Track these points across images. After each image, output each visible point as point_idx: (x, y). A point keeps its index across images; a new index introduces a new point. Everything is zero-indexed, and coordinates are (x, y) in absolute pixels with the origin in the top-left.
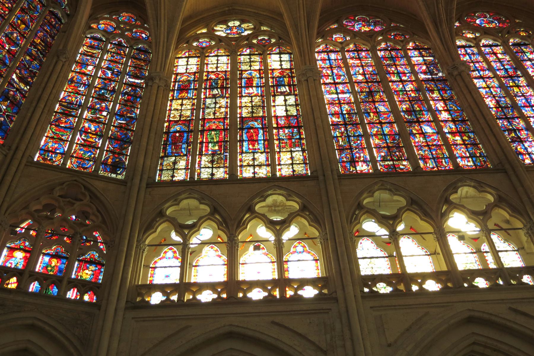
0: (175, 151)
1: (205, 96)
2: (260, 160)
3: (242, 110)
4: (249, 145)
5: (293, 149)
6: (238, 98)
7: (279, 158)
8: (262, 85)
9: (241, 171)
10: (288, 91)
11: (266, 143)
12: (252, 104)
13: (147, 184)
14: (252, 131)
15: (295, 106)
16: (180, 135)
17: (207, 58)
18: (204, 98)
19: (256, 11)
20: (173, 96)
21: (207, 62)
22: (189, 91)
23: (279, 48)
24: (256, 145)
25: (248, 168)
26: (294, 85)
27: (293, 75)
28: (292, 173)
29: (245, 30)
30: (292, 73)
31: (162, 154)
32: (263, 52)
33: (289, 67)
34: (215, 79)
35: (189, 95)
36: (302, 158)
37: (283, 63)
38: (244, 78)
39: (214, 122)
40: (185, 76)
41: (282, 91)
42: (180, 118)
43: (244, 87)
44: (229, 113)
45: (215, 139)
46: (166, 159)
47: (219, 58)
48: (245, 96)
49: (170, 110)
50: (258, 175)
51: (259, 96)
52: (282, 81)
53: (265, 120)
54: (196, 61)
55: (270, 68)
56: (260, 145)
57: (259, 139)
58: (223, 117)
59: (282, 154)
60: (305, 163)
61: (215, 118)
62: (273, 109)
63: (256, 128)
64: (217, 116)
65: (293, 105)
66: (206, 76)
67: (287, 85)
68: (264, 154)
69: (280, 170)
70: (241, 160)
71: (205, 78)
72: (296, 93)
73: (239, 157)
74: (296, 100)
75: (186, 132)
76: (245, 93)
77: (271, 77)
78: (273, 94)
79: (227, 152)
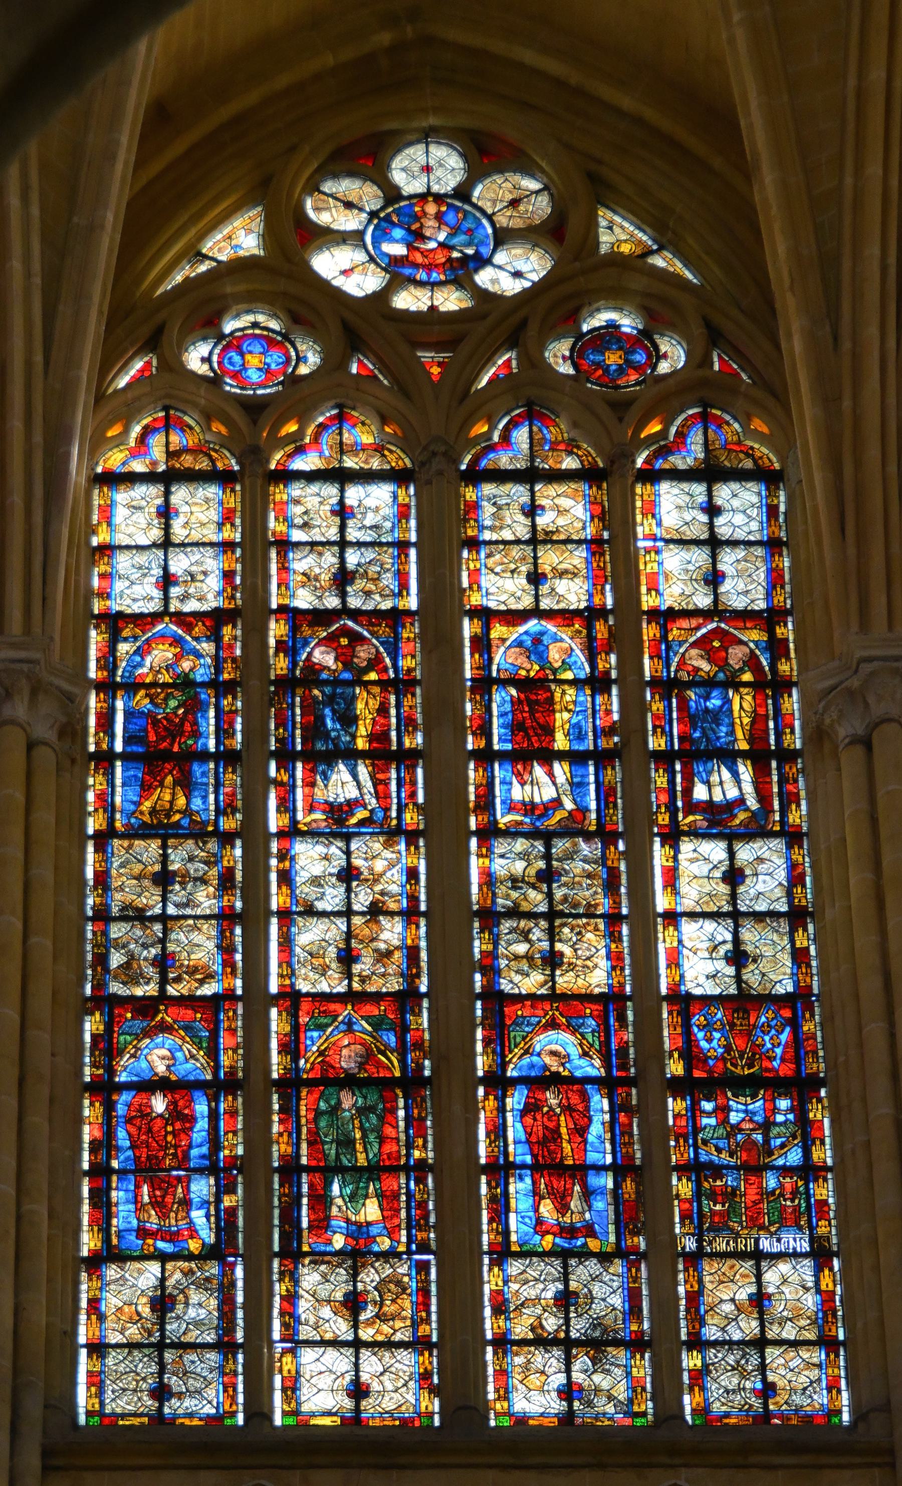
0: (153, 1221)
1: (286, 820)
2: (598, 1308)
3: (496, 944)
4: (536, 1193)
5: (766, 1244)
6: (474, 842)
7: (694, 1298)
8: (603, 743)
9: (502, 1373)
10: (752, 803)
11: (629, 1186)
12: (550, 895)
13: (47, 1453)
14: (552, 1099)
15: (784, 926)
16: (173, 1107)
17: (280, 494)
18: (281, 834)
19: (575, 78)
20: (106, 803)
21: (281, 528)
22: (197, 769)
23: (705, 418)
24: (575, 1204)
25: (539, 1358)
26: (787, 756)
27: (784, 667)
28: (756, 1403)
29: (502, 238)
30: (777, 649)
31: (89, 1242)
32: (611, 461)
33: (761, 605)
34: (337, 682)
35: (197, 803)
36: (810, 1301)
37: (728, 560)
38: (504, 683)
39: (349, 1024)
40: (162, 637)
41: (718, 797)
42: (163, 982)
43: (502, 756)
44: (424, 955)
45: (359, 1147)
46: (111, 1272)
47: (354, 494)
48: (511, 833)
49: (102, 916)
50: (590, 1404)
51: (588, 836)
52: (715, 716)
53: (622, 1019)
54: (214, 515)
55: (648, 601)
56: (599, 1204)
57: (592, 1157)
58: (394, 985)
59: (709, 1267)
60: (827, 1343)
61: (349, 997)
62: (665, 940)
63: (572, 1080)
64: (363, 980)
65: (773, 914)
66: (281, 646)
67: (744, 755)
68: (618, 1266)
69: (699, 1377)
70: (500, 1307)
71: (280, 665)
72: (794, 818)
73: (491, 1281)
74: (795, 879)
75: (200, 1085)
76: (511, 807)
77: (655, 683)
78: (664, 819)
79: (424, 1248)
